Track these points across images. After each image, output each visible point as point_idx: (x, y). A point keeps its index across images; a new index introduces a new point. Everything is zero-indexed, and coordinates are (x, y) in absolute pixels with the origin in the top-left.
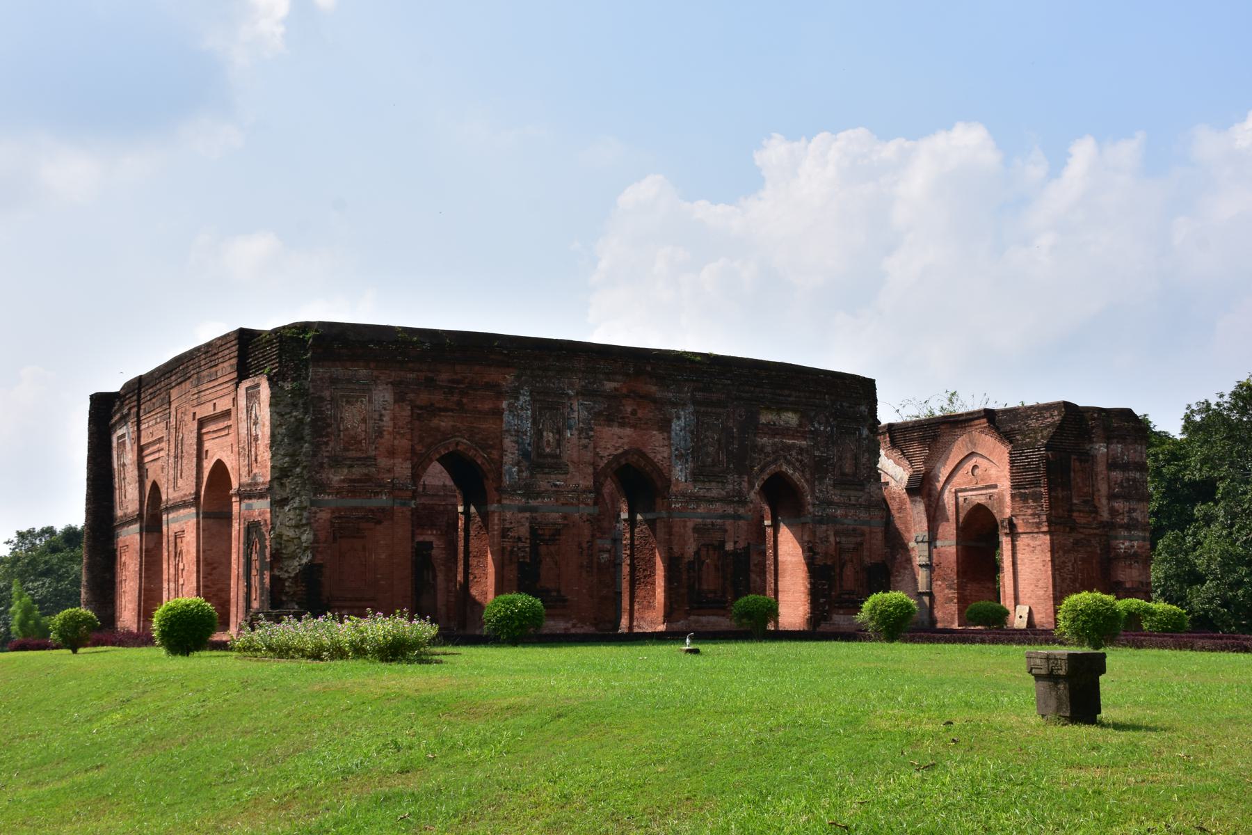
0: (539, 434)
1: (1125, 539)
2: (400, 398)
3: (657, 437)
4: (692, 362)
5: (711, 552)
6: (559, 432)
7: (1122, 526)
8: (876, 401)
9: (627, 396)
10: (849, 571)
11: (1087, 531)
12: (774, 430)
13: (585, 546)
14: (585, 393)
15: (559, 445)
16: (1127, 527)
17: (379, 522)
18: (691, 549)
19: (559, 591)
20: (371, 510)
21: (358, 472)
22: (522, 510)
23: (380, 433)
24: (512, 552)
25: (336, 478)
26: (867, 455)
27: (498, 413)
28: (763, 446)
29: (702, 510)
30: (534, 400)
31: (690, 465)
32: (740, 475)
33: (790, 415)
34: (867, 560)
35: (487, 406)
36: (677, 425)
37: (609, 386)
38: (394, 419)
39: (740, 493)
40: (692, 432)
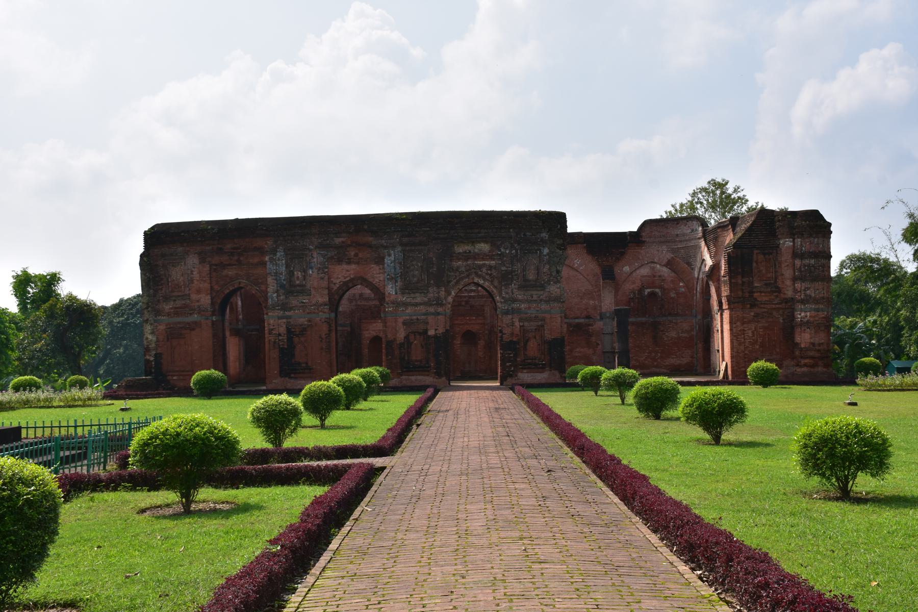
0: (291, 274)
1: (801, 310)
2: (202, 261)
3: (375, 269)
4: (397, 219)
5: (418, 337)
6: (305, 271)
7: (798, 301)
9: (350, 246)
10: (533, 345)
11: (769, 307)
12: (467, 256)
13: (324, 337)
14: (321, 247)
15: (304, 278)
16: (802, 302)
17: (194, 329)
18: (401, 335)
19: (307, 363)
20: (188, 323)
21: (179, 303)
22: (279, 318)
23: (192, 281)
24: (275, 342)
25: (167, 307)
26: (547, 266)
28: (458, 268)
29: (409, 310)
31: (399, 284)
32: (438, 287)
34: (548, 336)
35: (256, 260)
36: (388, 260)
37: (338, 241)
38: (199, 272)
39: (438, 299)
40: (400, 263)
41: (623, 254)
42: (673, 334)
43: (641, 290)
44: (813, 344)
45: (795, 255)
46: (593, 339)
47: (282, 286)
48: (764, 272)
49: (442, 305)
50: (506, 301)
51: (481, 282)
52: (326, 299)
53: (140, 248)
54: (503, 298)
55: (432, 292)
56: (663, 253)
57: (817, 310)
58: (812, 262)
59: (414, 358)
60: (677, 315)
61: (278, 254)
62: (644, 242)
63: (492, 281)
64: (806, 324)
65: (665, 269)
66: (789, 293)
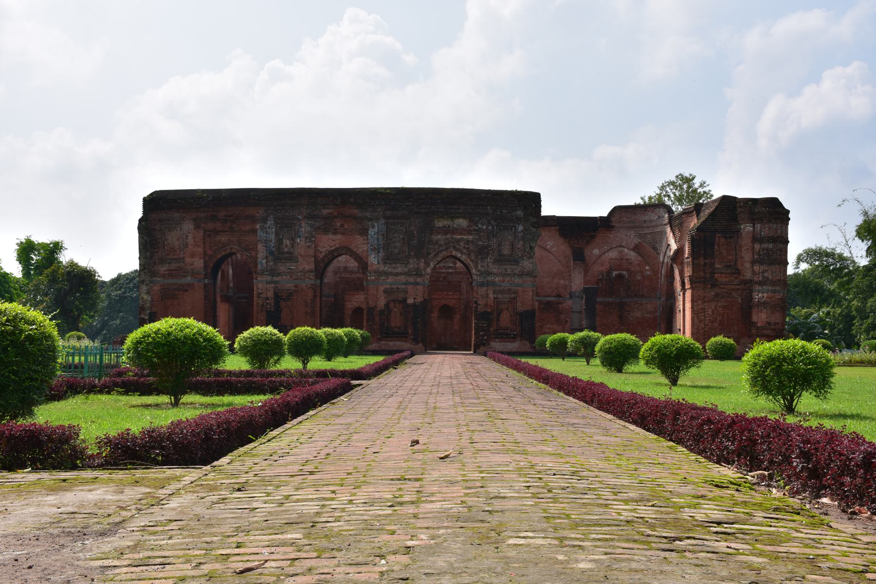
0: (280, 241)
1: (759, 292)
2: (197, 227)
4: (381, 193)
5: (397, 305)
7: (756, 283)
8: (541, 206)
12: (446, 231)
13: (309, 302)
14: (309, 217)
15: (293, 246)
16: (760, 283)
17: (187, 291)
18: (382, 303)
20: (182, 285)
21: (174, 266)
22: (268, 283)
23: (186, 245)
24: (263, 305)
25: (163, 269)
26: (521, 242)
27: (254, 231)
28: (438, 240)
29: (390, 279)
30: (276, 223)
31: (381, 254)
33: (461, 220)
34: (520, 309)
35: (247, 228)
36: (371, 232)
37: (325, 212)
38: (194, 238)
39: (418, 269)
40: (383, 235)
41: (593, 237)
42: (638, 314)
43: (609, 272)
44: (769, 323)
45: (755, 239)
46: (563, 316)
47: (271, 253)
48: (725, 254)
49: (421, 275)
50: (481, 274)
51: (459, 255)
52: (312, 266)
53: (139, 214)
54: (479, 271)
55: (412, 264)
56: (631, 238)
57: (774, 292)
58: (771, 246)
59: (393, 325)
60: (642, 296)
61: (269, 223)
62: (613, 227)
63: (469, 255)
64: (763, 304)
65: (632, 253)
66: (748, 275)
